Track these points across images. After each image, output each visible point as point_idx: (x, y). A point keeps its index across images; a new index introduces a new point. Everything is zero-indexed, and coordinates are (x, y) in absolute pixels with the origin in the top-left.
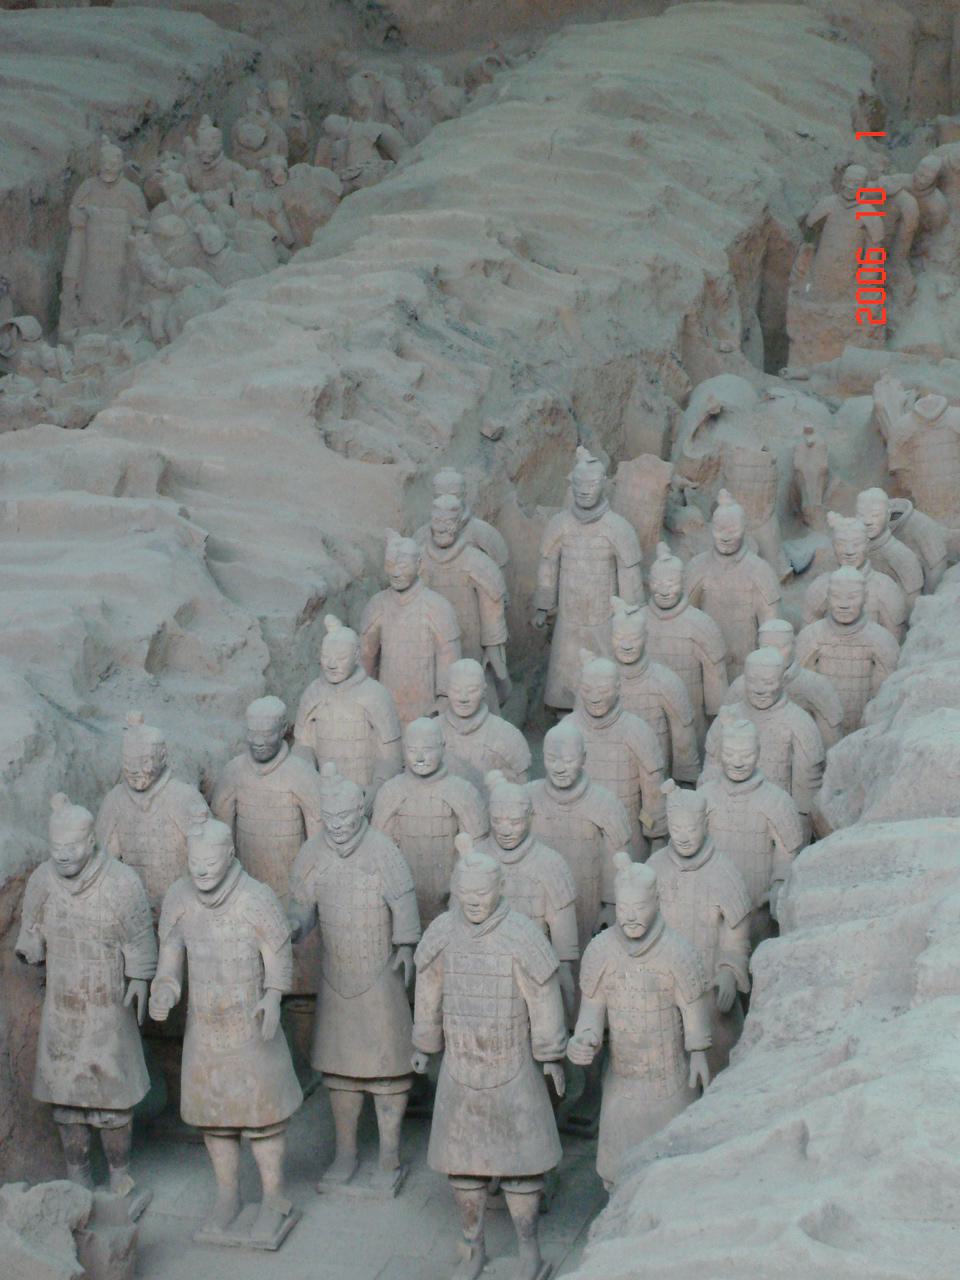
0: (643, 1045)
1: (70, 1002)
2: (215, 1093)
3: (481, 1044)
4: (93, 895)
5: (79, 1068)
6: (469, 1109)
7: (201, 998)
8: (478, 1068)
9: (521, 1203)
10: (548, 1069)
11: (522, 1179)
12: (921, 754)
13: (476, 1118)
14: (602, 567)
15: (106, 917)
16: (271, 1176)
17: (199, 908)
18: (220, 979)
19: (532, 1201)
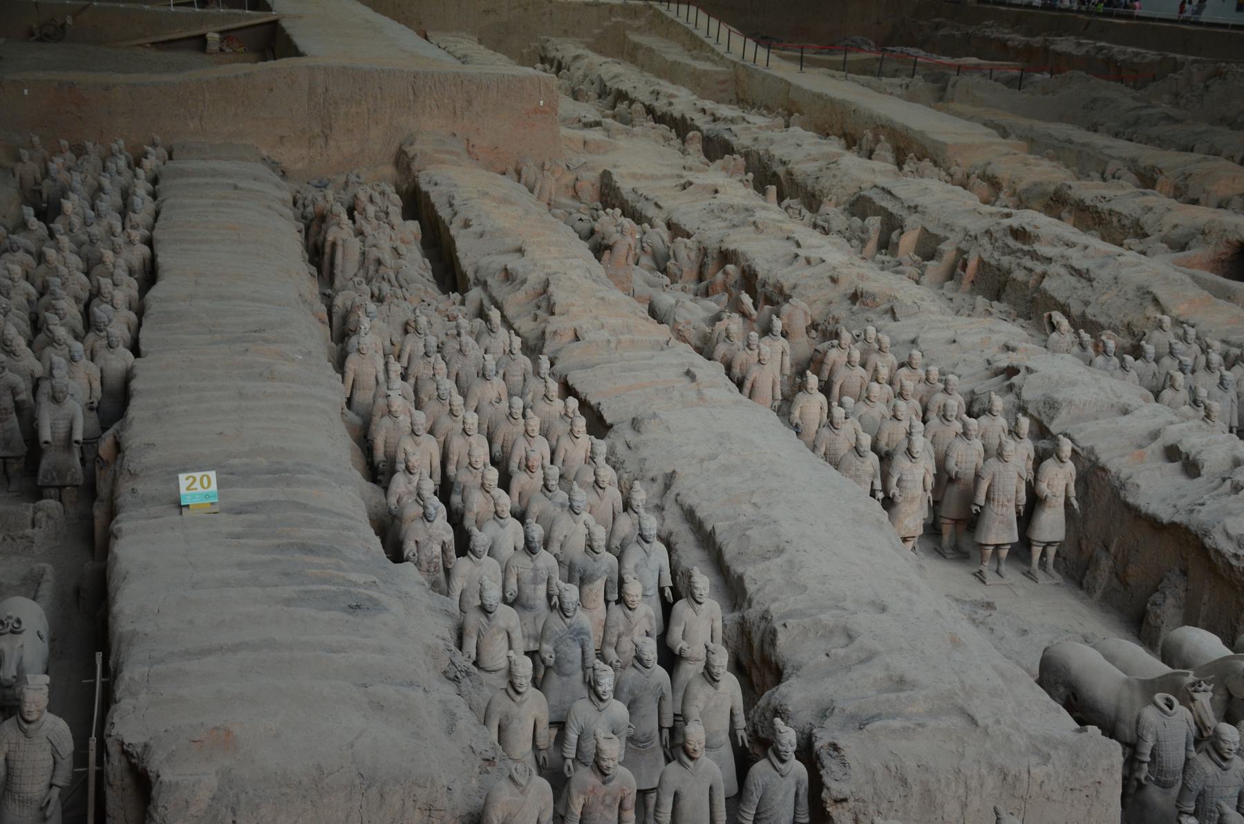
0: (1060, 496)
2: (906, 526)
3: (1008, 501)
4: (868, 463)
6: (1000, 523)
8: (1005, 509)
9: (1004, 553)
10: (1021, 508)
11: (1008, 544)
12: (1070, 402)
13: (1001, 525)
14: (780, 356)
15: (871, 470)
17: (909, 464)
18: (915, 487)
19: (1007, 551)
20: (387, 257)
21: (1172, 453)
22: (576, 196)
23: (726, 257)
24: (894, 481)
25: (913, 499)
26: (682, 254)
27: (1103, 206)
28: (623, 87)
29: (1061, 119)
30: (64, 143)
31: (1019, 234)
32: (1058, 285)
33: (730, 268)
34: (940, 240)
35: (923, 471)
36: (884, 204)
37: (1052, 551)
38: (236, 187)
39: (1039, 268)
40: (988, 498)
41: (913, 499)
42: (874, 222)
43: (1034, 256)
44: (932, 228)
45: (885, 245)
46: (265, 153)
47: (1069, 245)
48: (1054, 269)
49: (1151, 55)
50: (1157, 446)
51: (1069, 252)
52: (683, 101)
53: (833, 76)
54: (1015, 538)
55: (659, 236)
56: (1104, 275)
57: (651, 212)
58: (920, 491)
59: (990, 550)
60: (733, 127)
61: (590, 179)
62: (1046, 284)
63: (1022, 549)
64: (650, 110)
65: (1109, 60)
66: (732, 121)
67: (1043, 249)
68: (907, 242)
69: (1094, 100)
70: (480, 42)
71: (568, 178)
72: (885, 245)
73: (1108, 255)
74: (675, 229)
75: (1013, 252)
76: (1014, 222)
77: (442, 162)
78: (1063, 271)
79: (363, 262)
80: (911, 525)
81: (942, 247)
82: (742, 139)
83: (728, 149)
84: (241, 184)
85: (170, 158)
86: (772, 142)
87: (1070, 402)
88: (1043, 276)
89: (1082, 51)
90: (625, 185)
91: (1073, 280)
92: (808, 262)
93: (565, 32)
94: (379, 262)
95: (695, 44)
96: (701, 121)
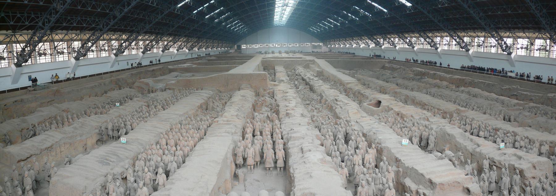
1: (239, 157)
5: (239, 161)
7: (249, 156)
16: (252, 168)
20: (215, 107)
21: (302, 149)
22: (269, 94)
23: (278, 106)
24: (246, 153)
25: (250, 157)
26: (274, 105)
27: (364, 94)
28: (301, 74)
29: (372, 77)
30: (184, 88)
31: (336, 100)
32: (338, 111)
33: (277, 108)
34: (327, 101)
35: (252, 151)
36: (323, 94)
37: (282, 169)
38: (200, 95)
39: (336, 106)
40: (266, 158)
41: (250, 157)
42: (319, 97)
43: (337, 104)
44: (327, 99)
45: (320, 102)
46: (218, 88)
47: (342, 102)
48: (338, 107)
49: (399, 67)
50: (300, 147)
51: (341, 103)
52: (308, 75)
53: (340, 71)
54: (273, 165)
55: (273, 101)
56: (343, 108)
57: (275, 97)
58: (251, 156)
59: (268, 169)
60: (311, 80)
61: (271, 90)
62: (336, 110)
63: (276, 167)
64: (302, 78)
65: (393, 68)
66: (312, 79)
67: (338, 103)
68: (323, 101)
69: (383, 74)
70: (284, 67)
71: (268, 91)
72: (320, 102)
73: (347, 104)
74: (276, 101)
75: (335, 103)
76: (337, 98)
77: (245, 89)
78: (339, 107)
79: (212, 108)
80: (251, 162)
81: (327, 102)
82: (311, 83)
83: (309, 85)
84: (201, 94)
85: (202, 90)
86: (315, 83)
87: (293, 137)
88: (336, 108)
89: (389, 66)
90: (275, 92)
91: (340, 109)
92: (287, 106)
93: (299, 65)
94: (214, 108)
95: (319, 66)
96: (308, 80)
